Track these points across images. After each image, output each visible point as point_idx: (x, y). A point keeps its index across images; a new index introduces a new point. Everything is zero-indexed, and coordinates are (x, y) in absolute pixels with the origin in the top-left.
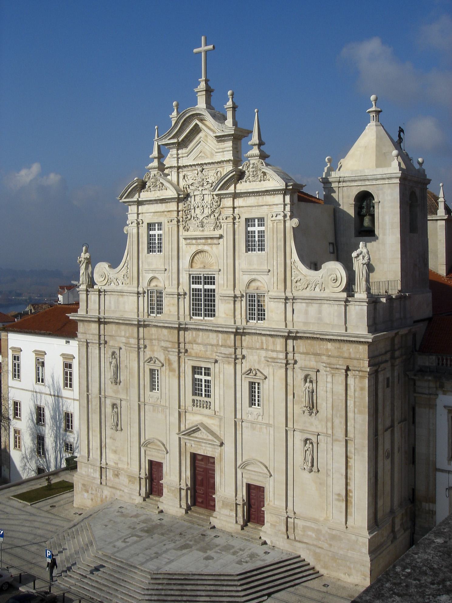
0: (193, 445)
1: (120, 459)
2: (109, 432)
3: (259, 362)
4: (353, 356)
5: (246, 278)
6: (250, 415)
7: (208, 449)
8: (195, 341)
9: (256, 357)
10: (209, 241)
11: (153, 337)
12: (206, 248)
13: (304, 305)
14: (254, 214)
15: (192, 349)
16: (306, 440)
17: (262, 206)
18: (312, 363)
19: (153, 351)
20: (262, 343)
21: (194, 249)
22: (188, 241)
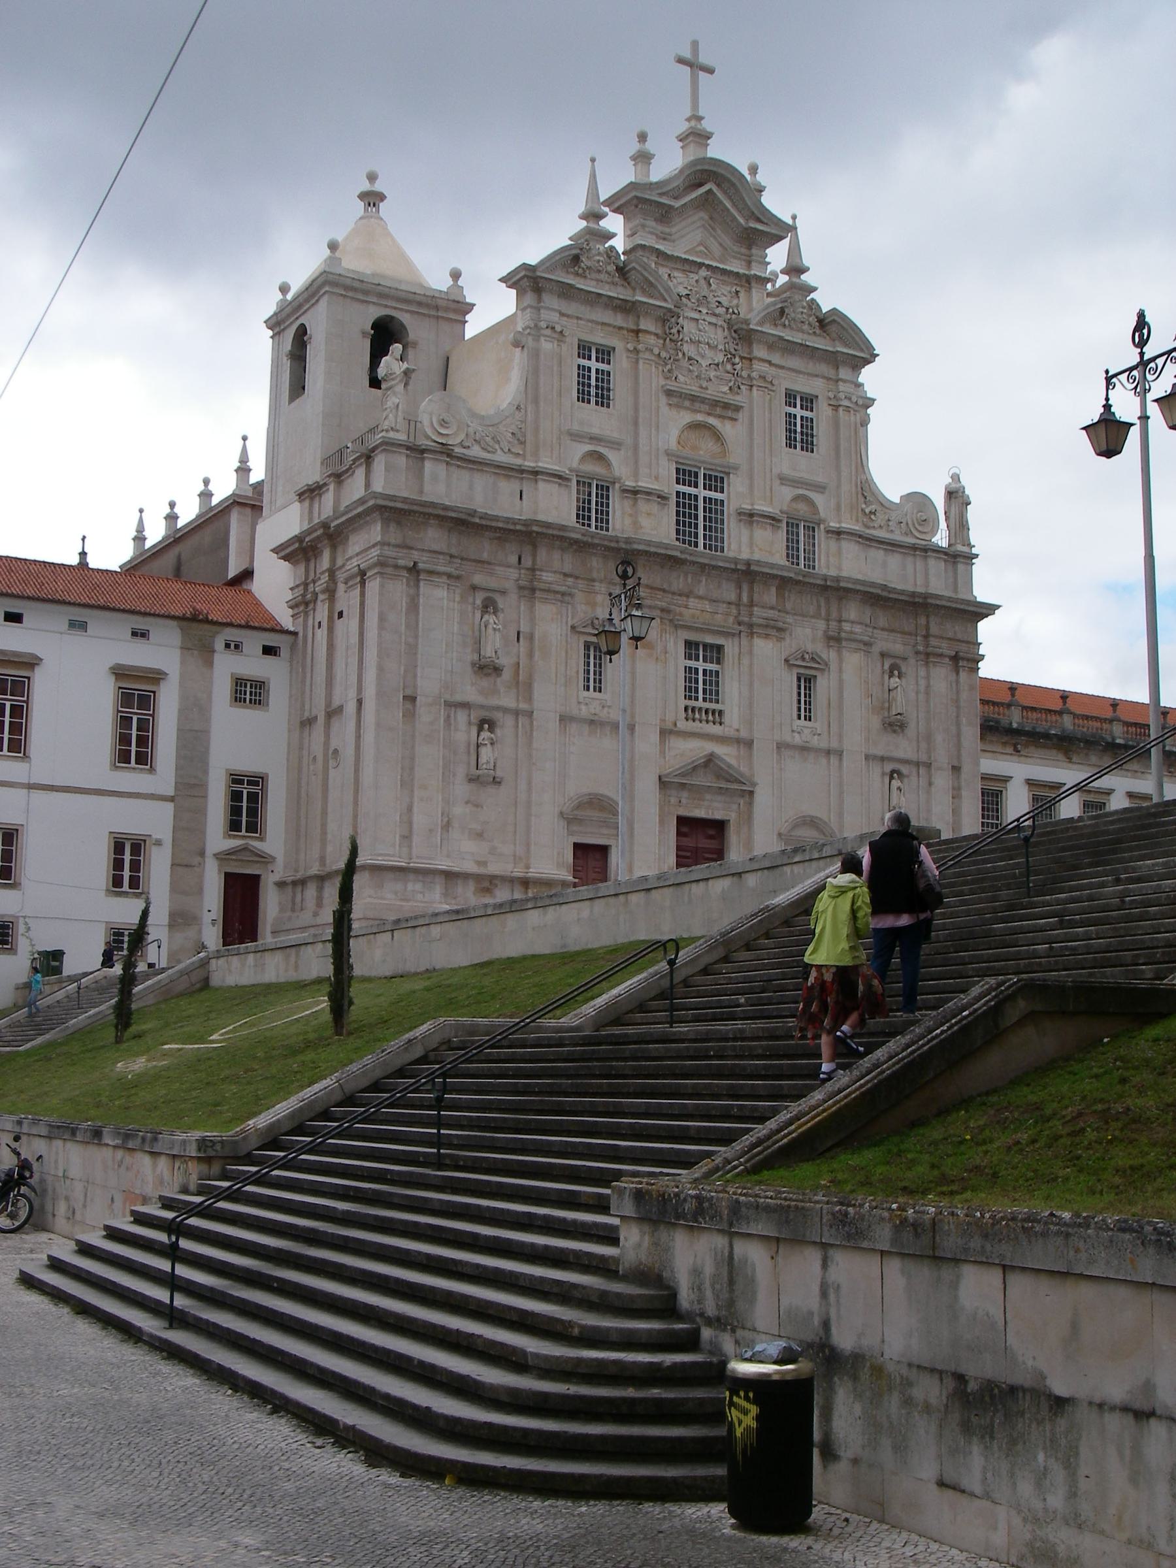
0: (684, 801)
1: (493, 851)
2: (461, 789)
3: (814, 640)
4: (959, 636)
5: (788, 493)
6: (796, 735)
7: (715, 804)
8: (691, 592)
9: (808, 631)
10: (718, 411)
11: (595, 575)
12: (712, 421)
13: (882, 552)
14: (803, 385)
15: (686, 607)
16: (893, 772)
17: (817, 376)
18: (897, 645)
19: (593, 605)
20: (819, 606)
21: (687, 417)
22: (675, 400)
